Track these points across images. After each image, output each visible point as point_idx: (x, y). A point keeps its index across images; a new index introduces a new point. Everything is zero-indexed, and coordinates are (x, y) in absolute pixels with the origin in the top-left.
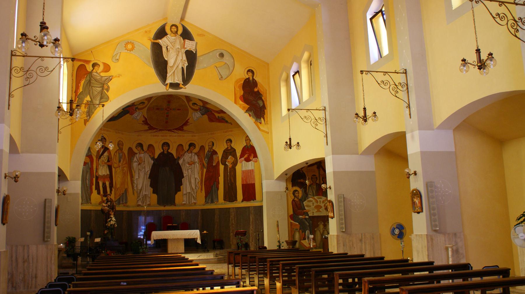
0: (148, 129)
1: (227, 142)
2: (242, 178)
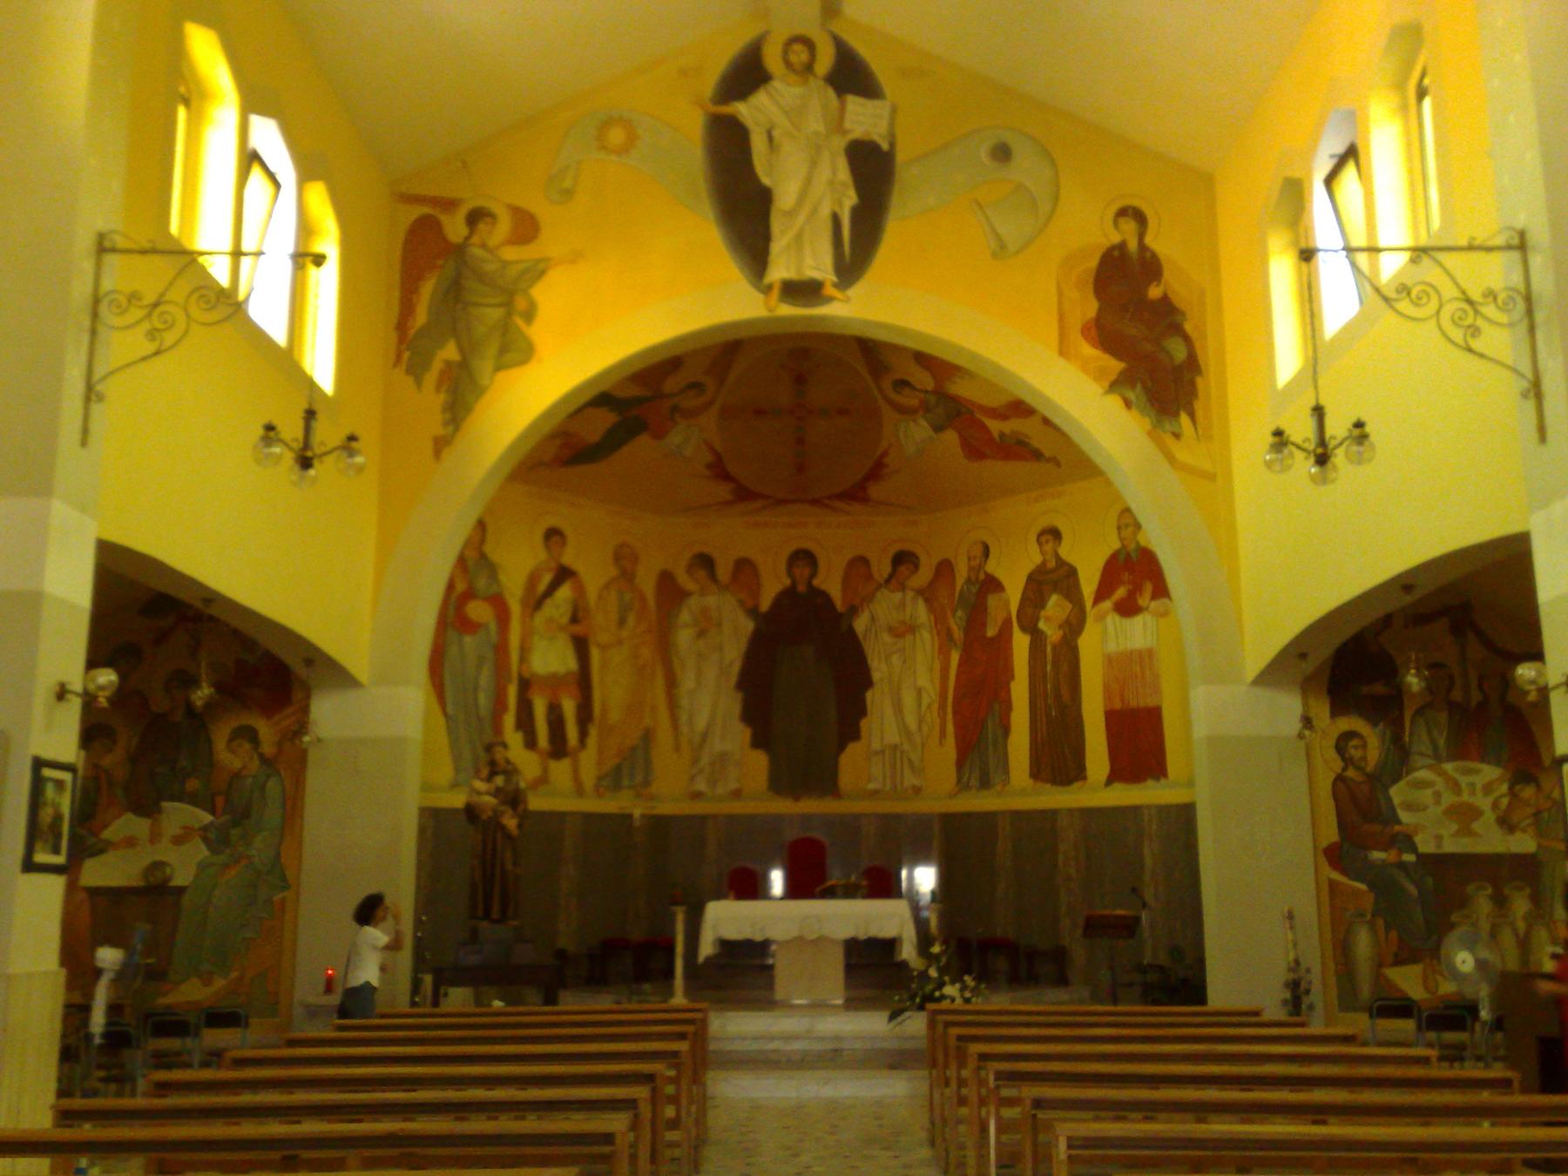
1: (1043, 539)
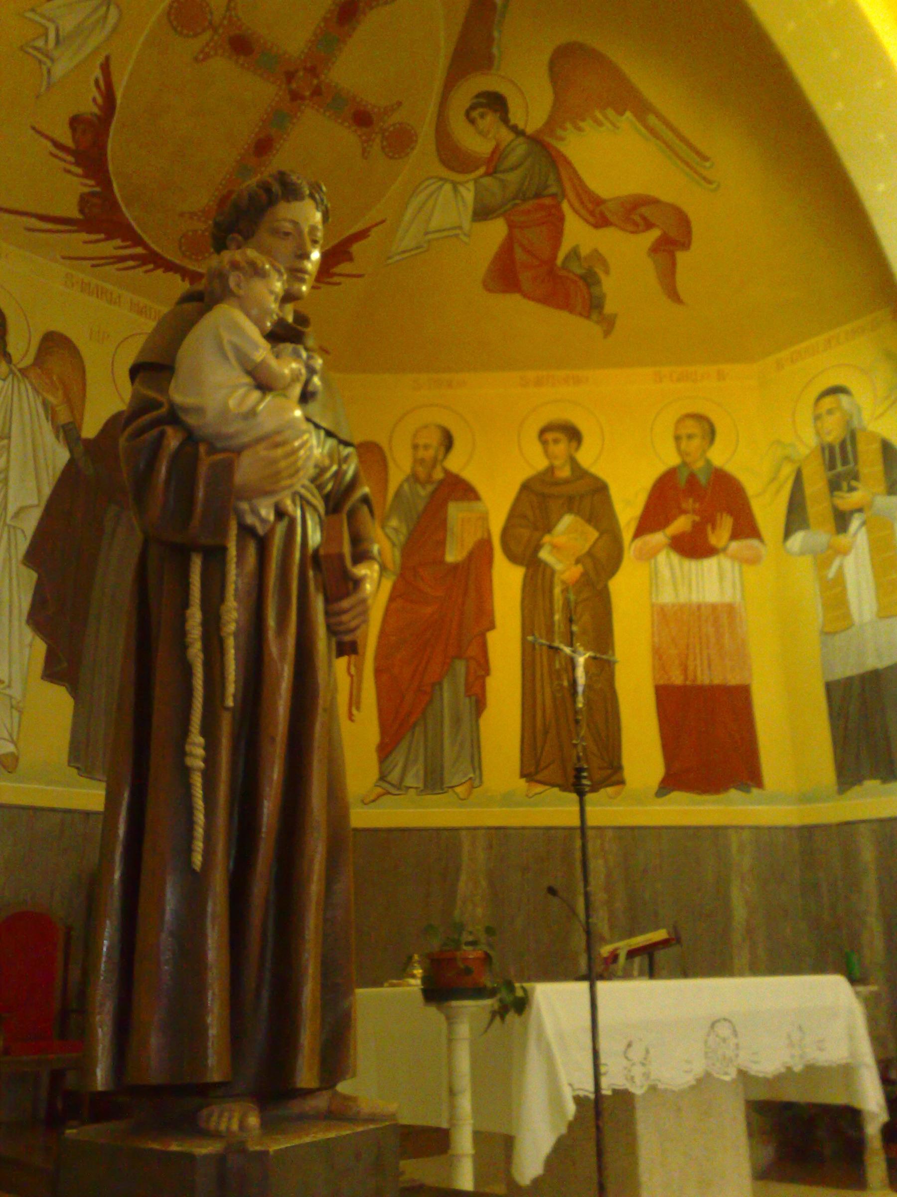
0: (75, 214)
1: (550, 436)
2: (657, 653)
